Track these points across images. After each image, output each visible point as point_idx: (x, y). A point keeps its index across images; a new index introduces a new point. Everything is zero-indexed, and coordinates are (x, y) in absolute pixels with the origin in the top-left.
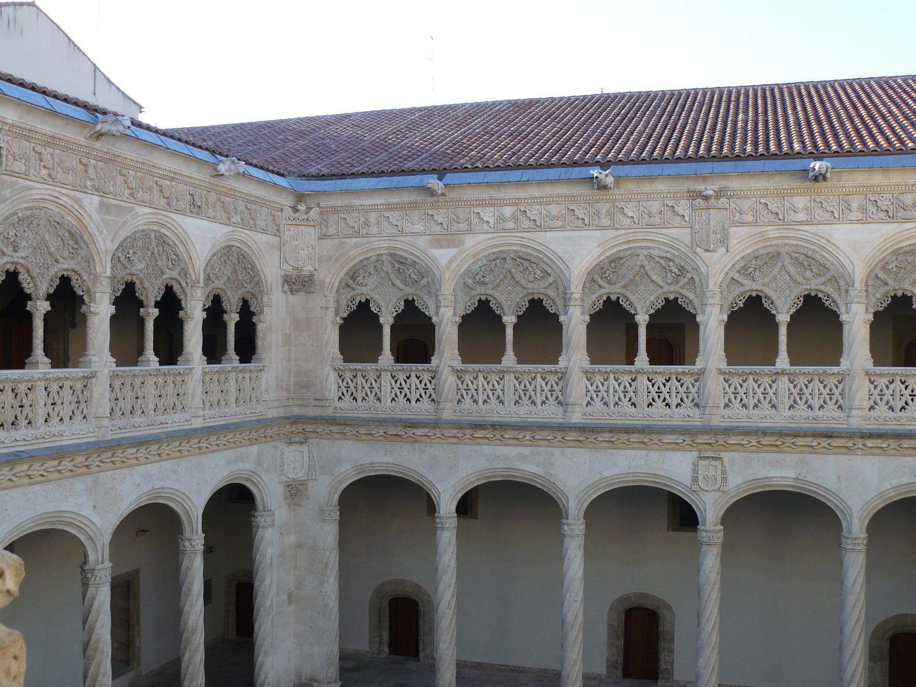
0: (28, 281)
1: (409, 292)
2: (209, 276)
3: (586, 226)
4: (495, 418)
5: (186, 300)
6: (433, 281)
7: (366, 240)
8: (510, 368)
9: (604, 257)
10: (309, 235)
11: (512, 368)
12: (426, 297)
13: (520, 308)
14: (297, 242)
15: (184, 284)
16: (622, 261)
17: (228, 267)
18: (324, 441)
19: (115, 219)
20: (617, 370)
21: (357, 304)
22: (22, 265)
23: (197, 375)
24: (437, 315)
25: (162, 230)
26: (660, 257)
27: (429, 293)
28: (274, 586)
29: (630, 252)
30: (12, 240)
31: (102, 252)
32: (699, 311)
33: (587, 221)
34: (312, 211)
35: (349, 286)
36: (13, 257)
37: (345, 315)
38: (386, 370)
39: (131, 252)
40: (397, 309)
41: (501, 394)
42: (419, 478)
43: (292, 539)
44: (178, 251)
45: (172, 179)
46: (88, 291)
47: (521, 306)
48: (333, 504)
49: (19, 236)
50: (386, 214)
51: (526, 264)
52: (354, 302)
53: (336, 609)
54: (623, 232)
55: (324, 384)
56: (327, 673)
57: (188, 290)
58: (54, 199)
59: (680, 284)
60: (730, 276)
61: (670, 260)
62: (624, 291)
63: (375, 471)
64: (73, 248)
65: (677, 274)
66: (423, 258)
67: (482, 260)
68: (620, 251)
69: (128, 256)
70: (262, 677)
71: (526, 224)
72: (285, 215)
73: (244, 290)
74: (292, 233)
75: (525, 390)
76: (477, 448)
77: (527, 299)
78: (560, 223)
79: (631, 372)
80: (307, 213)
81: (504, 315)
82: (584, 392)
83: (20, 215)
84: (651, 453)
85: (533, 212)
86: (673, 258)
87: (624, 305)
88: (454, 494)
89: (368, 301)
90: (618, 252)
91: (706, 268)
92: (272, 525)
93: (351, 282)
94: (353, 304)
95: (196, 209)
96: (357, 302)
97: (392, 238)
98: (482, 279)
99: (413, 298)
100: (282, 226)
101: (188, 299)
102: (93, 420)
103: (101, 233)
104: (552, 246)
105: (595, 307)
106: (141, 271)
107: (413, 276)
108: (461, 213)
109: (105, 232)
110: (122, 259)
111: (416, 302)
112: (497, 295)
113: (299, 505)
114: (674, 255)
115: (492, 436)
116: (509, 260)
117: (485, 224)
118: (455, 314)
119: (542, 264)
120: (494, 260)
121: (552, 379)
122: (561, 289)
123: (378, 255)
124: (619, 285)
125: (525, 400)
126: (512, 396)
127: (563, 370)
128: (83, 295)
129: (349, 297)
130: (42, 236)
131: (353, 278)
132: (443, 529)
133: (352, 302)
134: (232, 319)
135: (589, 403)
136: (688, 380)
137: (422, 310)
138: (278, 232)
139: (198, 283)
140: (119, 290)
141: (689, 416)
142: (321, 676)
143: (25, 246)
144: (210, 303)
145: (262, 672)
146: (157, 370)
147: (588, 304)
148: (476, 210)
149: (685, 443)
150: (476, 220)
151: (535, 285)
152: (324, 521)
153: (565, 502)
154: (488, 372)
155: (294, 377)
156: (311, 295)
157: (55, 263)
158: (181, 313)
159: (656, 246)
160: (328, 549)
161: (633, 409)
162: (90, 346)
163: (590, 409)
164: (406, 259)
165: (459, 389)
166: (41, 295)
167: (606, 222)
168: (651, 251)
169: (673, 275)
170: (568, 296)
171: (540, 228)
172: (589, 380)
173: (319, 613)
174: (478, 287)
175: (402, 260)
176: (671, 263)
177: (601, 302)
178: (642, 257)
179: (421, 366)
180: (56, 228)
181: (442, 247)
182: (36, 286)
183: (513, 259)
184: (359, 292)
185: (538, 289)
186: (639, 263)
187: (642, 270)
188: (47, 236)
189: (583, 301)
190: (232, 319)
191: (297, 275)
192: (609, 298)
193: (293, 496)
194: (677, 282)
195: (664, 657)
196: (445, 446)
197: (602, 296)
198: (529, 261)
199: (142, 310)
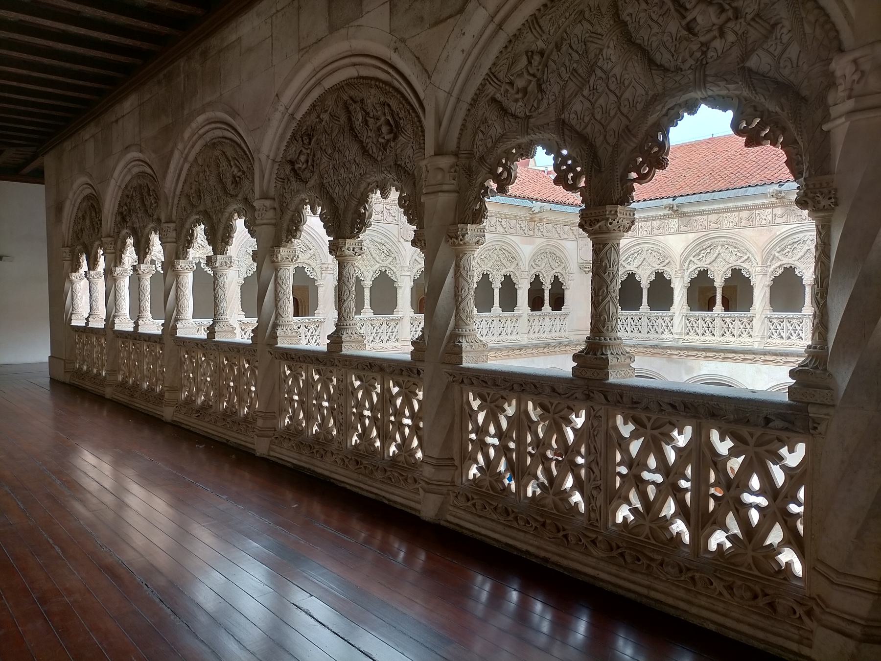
32: (399, 280)
60: (414, 258)
65: (387, 254)
86: (386, 244)
91: (404, 251)
127: (323, 320)
136: (312, 327)
159: (375, 234)
176: (384, 247)
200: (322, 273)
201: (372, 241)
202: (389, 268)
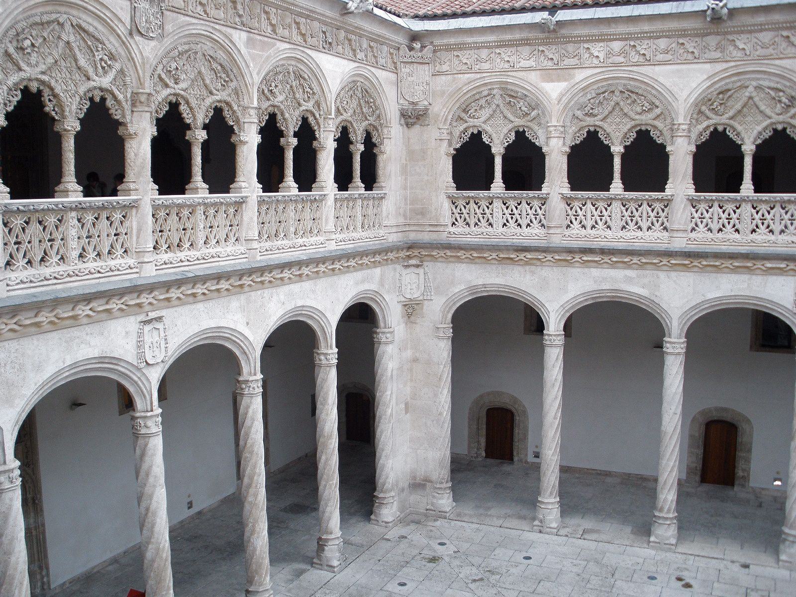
1: (519, 122)
2: (338, 109)
3: (696, 59)
4: (603, 244)
5: (319, 131)
6: (543, 113)
7: (478, 76)
8: (617, 195)
9: (712, 89)
10: (423, 73)
11: (620, 195)
12: (536, 128)
13: (628, 138)
14: (412, 78)
15: (318, 116)
16: (729, 93)
17: (354, 101)
18: (439, 264)
20: (723, 197)
21: (469, 135)
23: (330, 201)
24: (547, 144)
25: (299, 65)
26: (769, 88)
27: (540, 124)
28: (394, 396)
29: (739, 84)
30: (174, 72)
33: (697, 54)
34: (426, 49)
35: (461, 119)
37: (458, 146)
38: (498, 197)
39: (273, 84)
40: (508, 139)
41: (609, 220)
42: (529, 298)
43: (408, 354)
44: (313, 85)
45: (307, 17)
46: (237, 121)
47: (628, 136)
48: (447, 322)
50: (498, 51)
51: (634, 96)
52: (466, 134)
53: (449, 417)
54: (733, 64)
55: (439, 210)
56: (440, 474)
57: (321, 121)
58: (208, 34)
59: (790, 114)
61: (780, 91)
62: (732, 122)
63: (487, 291)
64: (225, 81)
66: (534, 92)
67: (591, 93)
68: (729, 83)
69: (270, 88)
70: (384, 477)
71: (636, 58)
72: (401, 53)
73: (367, 122)
74: (407, 70)
75: (632, 216)
76: (586, 270)
77: (635, 130)
78: (669, 57)
79: (736, 199)
80: (421, 51)
81: (613, 145)
82: (689, 218)
83: (180, 49)
84: (754, 277)
85: (643, 46)
86: (784, 89)
87: (731, 136)
88: (562, 313)
89: (480, 133)
90: (727, 84)
92: (392, 342)
93: (463, 115)
94: (466, 136)
95: (328, 47)
96: (470, 133)
97: (503, 73)
98: (591, 111)
99: (524, 130)
100: (398, 63)
101: (322, 130)
102: (244, 242)
104: (661, 79)
105: (702, 137)
106: (282, 102)
107: (524, 108)
108: (570, 47)
109: (252, 65)
110: (266, 91)
111: (527, 133)
112: (605, 126)
113: (415, 323)
114: (786, 86)
115: (600, 259)
116: (617, 93)
117: (594, 59)
118: (564, 144)
119: (650, 96)
120: (603, 93)
121: (658, 206)
122: (668, 121)
123: (490, 89)
124: (727, 116)
125: (632, 225)
126: (619, 221)
128: (233, 126)
129: (462, 128)
130: (199, 70)
131: (465, 111)
132: (551, 346)
133: (464, 134)
134: (358, 148)
135: (693, 229)
137: (533, 141)
138: (395, 70)
139: (330, 114)
140: (263, 121)
141: (793, 242)
142: (434, 477)
143: (184, 79)
144: (339, 134)
145: (384, 473)
146: (296, 196)
147: (694, 136)
148: (586, 46)
149: (789, 268)
150: (587, 55)
151: (643, 117)
152: (438, 338)
153: (668, 322)
154: (597, 200)
155: (410, 205)
156: (425, 128)
158: (315, 144)
160: (442, 363)
161: (736, 235)
162: (240, 173)
163: (693, 235)
164: (517, 92)
165: (568, 215)
167: (718, 55)
168: (761, 82)
169: (783, 105)
170: (676, 127)
171: (648, 62)
172: (694, 207)
173: (433, 421)
174: (588, 119)
175: (513, 94)
176: (781, 94)
177: (708, 132)
178: (751, 89)
179: (531, 193)
180: (210, 62)
181: (552, 81)
183: (621, 92)
184: (471, 124)
185: (646, 120)
186: (747, 94)
187: (751, 101)
189: (689, 131)
190: (358, 148)
191: (413, 109)
192: (716, 129)
193: (409, 315)
194: (787, 112)
195: (740, 465)
196: (555, 268)
197: (708, 127)
198: (637, 93)
199: (282, 140)
200: (673, 137)
201: (758, 88)
202: (789, 124)
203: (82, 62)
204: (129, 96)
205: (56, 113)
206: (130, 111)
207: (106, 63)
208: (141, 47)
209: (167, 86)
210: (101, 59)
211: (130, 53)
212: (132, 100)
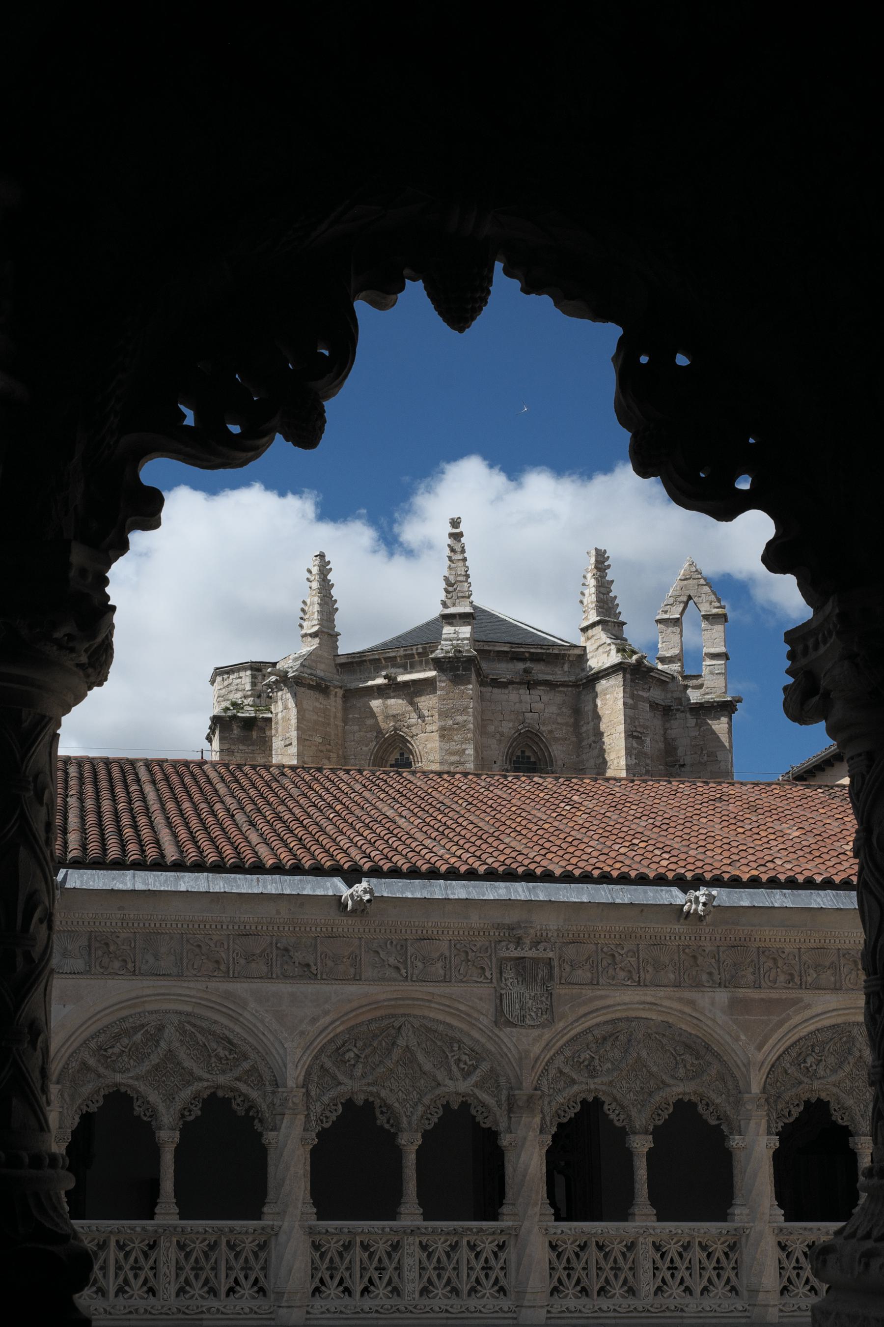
0: (617, 1112)
19: (762, 1018)
22: (604, 1093)
31: (744, 1065)
36: (587, 1083)
49: (597, 1057)
103: (737, 1039)
109: (743, 1037)
157: (662, 1086)
166: (638, 1127)
182: (629, 1117)
188: (644, 1054)
203: (428, 1067)
204: (504, 1098)
205: (392, 1126)
206: (506, 1119)
207: (465, 1063)
208: (514, 1039)
209: (573, 1082)
210: (459, 1060)
211: (501, 1049)
212: (509, 1104)
